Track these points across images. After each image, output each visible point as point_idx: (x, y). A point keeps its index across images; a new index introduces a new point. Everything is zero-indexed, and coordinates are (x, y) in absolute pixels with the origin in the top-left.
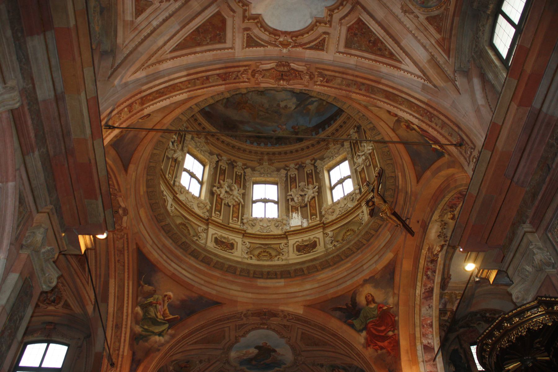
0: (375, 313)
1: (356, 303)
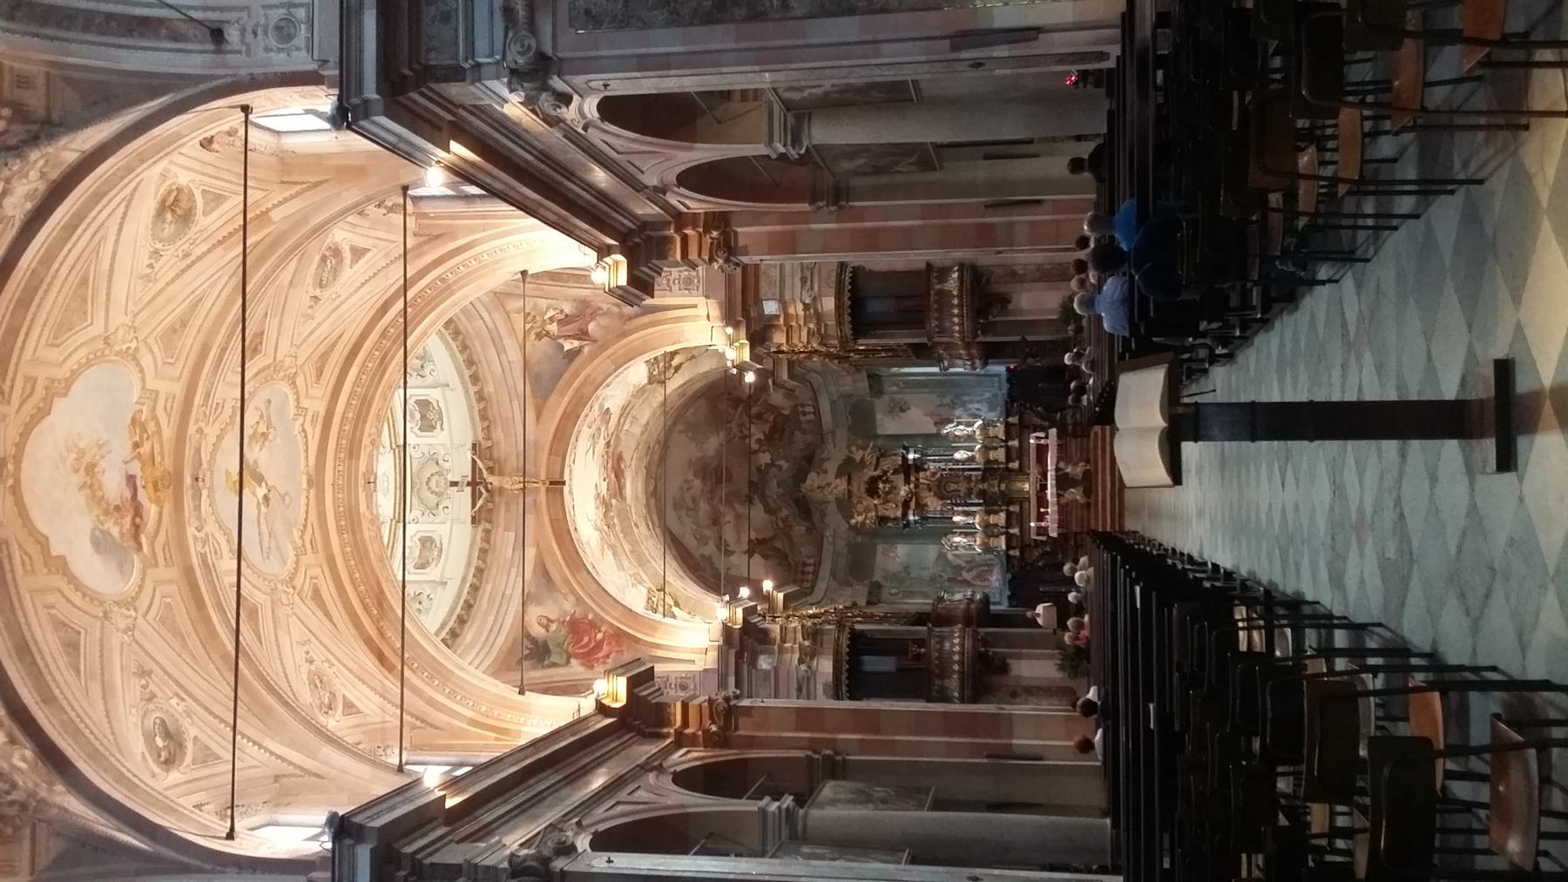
0: (563, 632)
1: (534, 638)
